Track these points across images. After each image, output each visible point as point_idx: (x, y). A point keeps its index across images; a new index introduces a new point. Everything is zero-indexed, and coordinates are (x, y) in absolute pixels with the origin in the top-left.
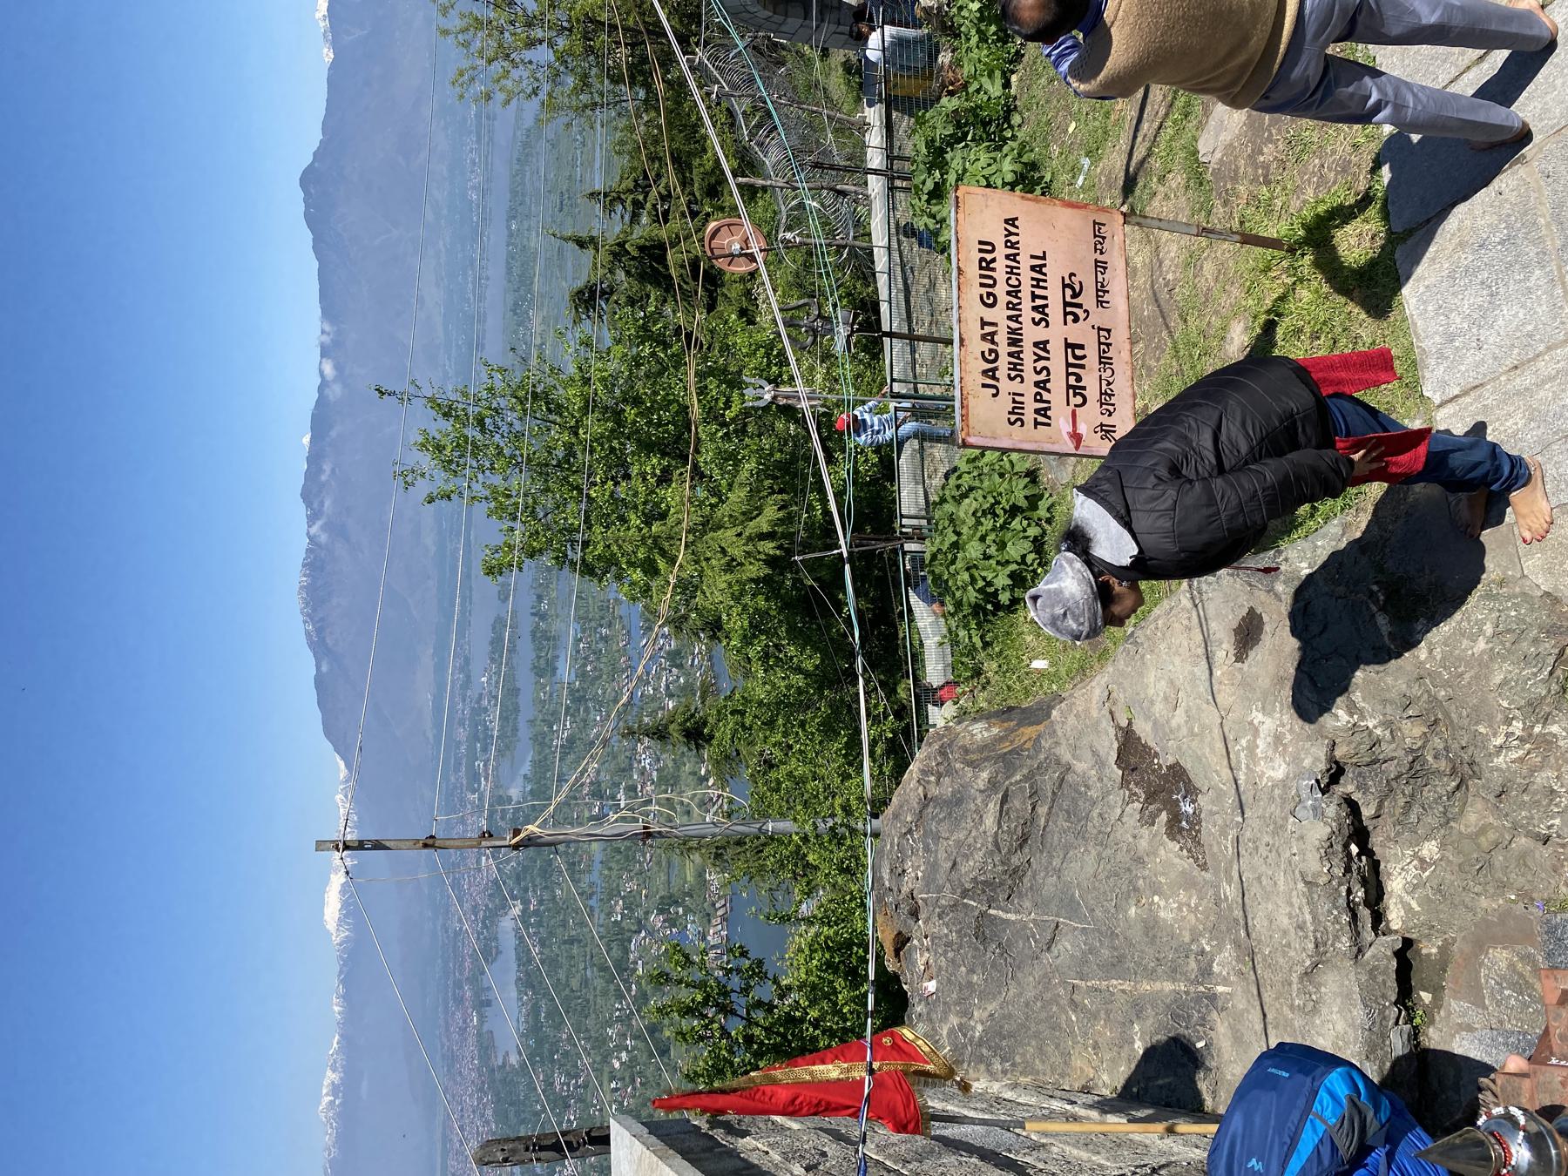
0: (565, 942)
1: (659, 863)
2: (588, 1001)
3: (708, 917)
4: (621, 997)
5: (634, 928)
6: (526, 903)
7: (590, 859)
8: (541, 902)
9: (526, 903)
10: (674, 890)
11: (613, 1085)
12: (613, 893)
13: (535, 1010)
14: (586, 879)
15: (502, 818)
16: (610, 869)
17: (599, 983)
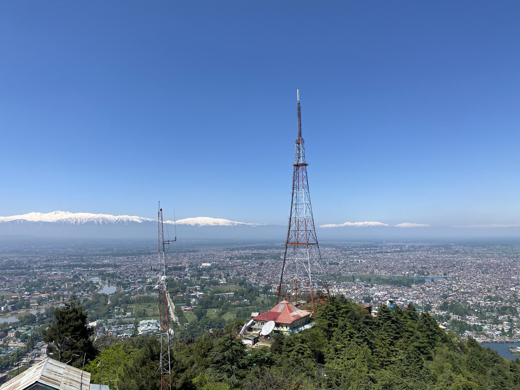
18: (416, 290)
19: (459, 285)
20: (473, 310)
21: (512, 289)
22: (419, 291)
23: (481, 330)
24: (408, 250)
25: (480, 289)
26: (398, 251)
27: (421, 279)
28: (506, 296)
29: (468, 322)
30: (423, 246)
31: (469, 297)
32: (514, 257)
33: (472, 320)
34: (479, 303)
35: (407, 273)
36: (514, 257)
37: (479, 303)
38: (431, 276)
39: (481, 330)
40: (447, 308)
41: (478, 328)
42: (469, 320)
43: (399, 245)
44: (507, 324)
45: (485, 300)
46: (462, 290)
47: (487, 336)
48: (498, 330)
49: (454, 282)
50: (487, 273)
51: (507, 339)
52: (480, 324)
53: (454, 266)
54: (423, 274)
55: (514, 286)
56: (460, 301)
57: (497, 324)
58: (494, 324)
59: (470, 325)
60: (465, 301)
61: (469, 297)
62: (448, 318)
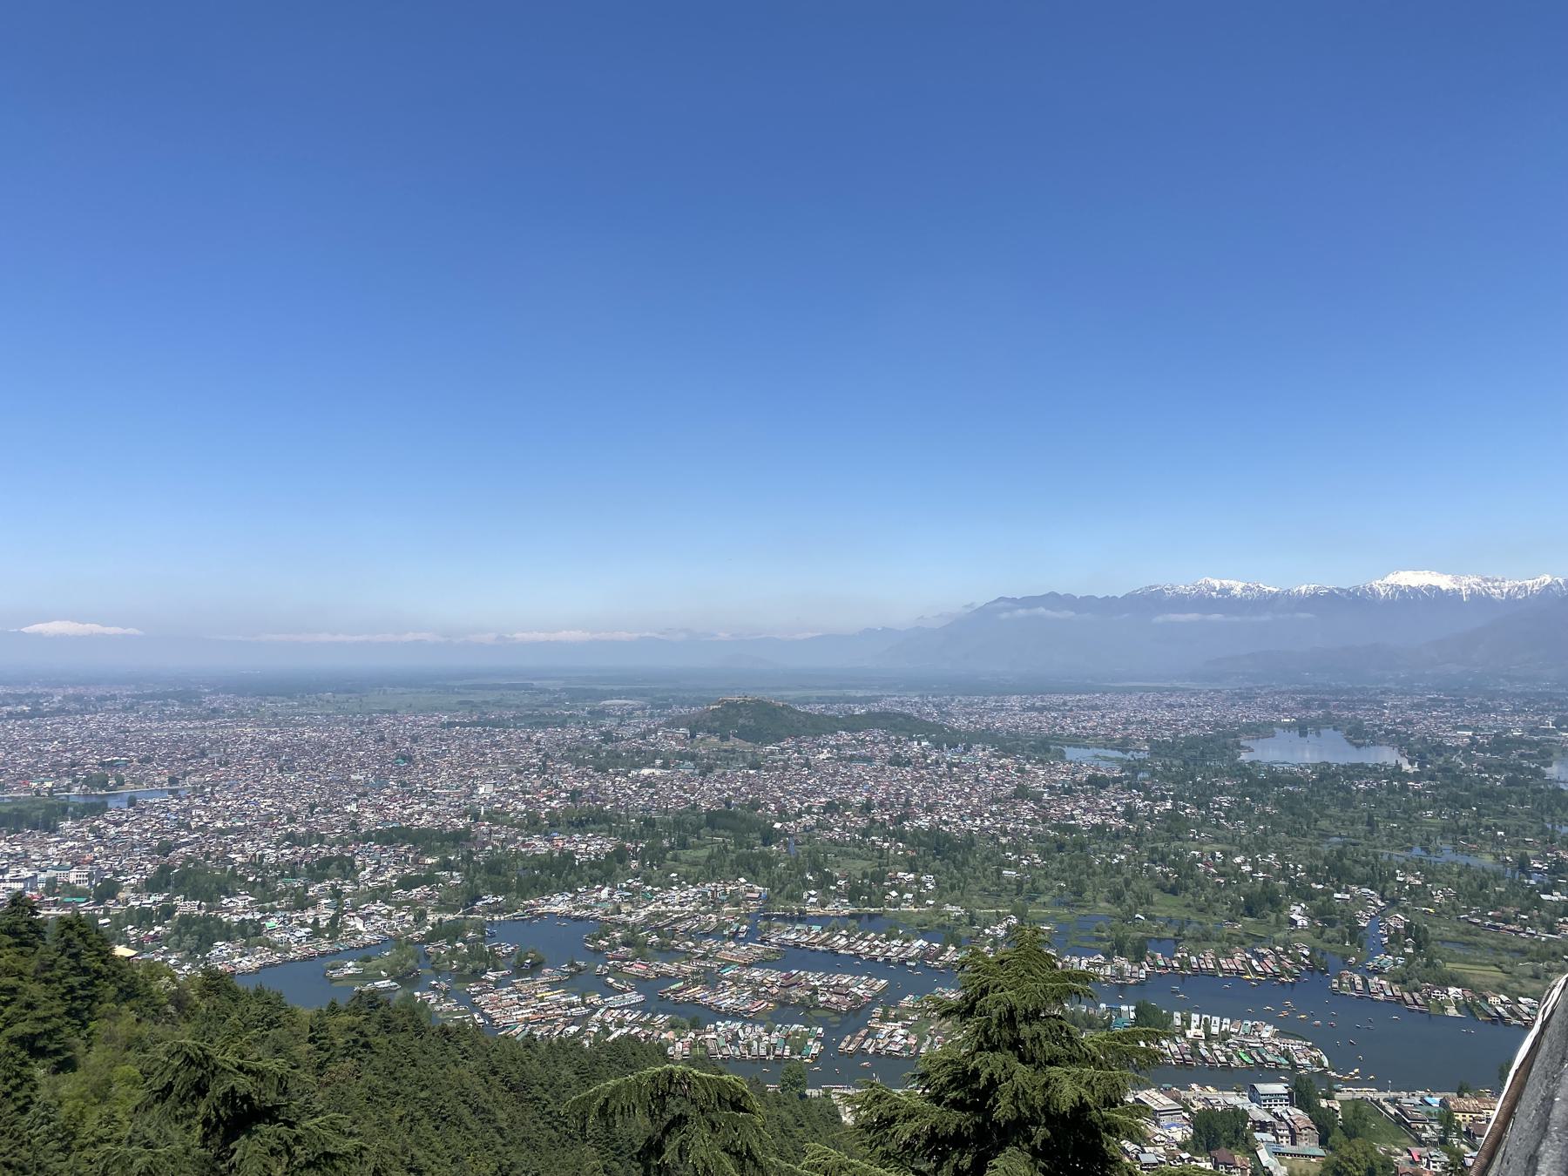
0: (1370, 817)
1: (1468, 932)
2: (1304, 836)
3: (1401, 980)
4: (1310, 870)
5: (1387, 893)
6: (1417, 777)
7: (1476, 852)
8: (1417, 793)
9: (1417, 777)
10: (1433, 946)
11: (1218, 854)
12: (1430, 875)
13: (1296, 781)
14: (1447, 846)
15: (1522, 756)
16: (1460, 874)
17: (1324, 849)
18: (73, 838)
19: (211, 809)
20: (243, 878)
21: (349, 808)
22: (83, 839)
23: (258, 934)
24: (60, 711)
25: (269, 817)
26: (23, 715)
27: (94, 800)
28: (332, 827)
29: (225, 917)
30: (113, 697)
31: (235, 841)
32: (363, 723)
33: (237, 908)
34: (262, 856)
35: (49, 784)
36: (363, 723)
37: (262, 856)
38: (128, 789)
39: (257, 934)
40: (168, 883)
41: (250, 930)
42: (229, 910)
43: (29, 695)
44: (327, 906)
45: (278, 844)
46: (219, 824)
47: (273, 947)
48: (303, 924)
49: (198, 801)
50: (292, 770)
51: (325, 946)
52: (258, 916)
53: (203, 754)
54: (104, 785)
55: (356, 800)
56: (207, 858)
57: (303, 909)
58: (295, 910)
59: (229, 925)
60: (225, 853)
61: (235, 841)
62: (168, 911)
